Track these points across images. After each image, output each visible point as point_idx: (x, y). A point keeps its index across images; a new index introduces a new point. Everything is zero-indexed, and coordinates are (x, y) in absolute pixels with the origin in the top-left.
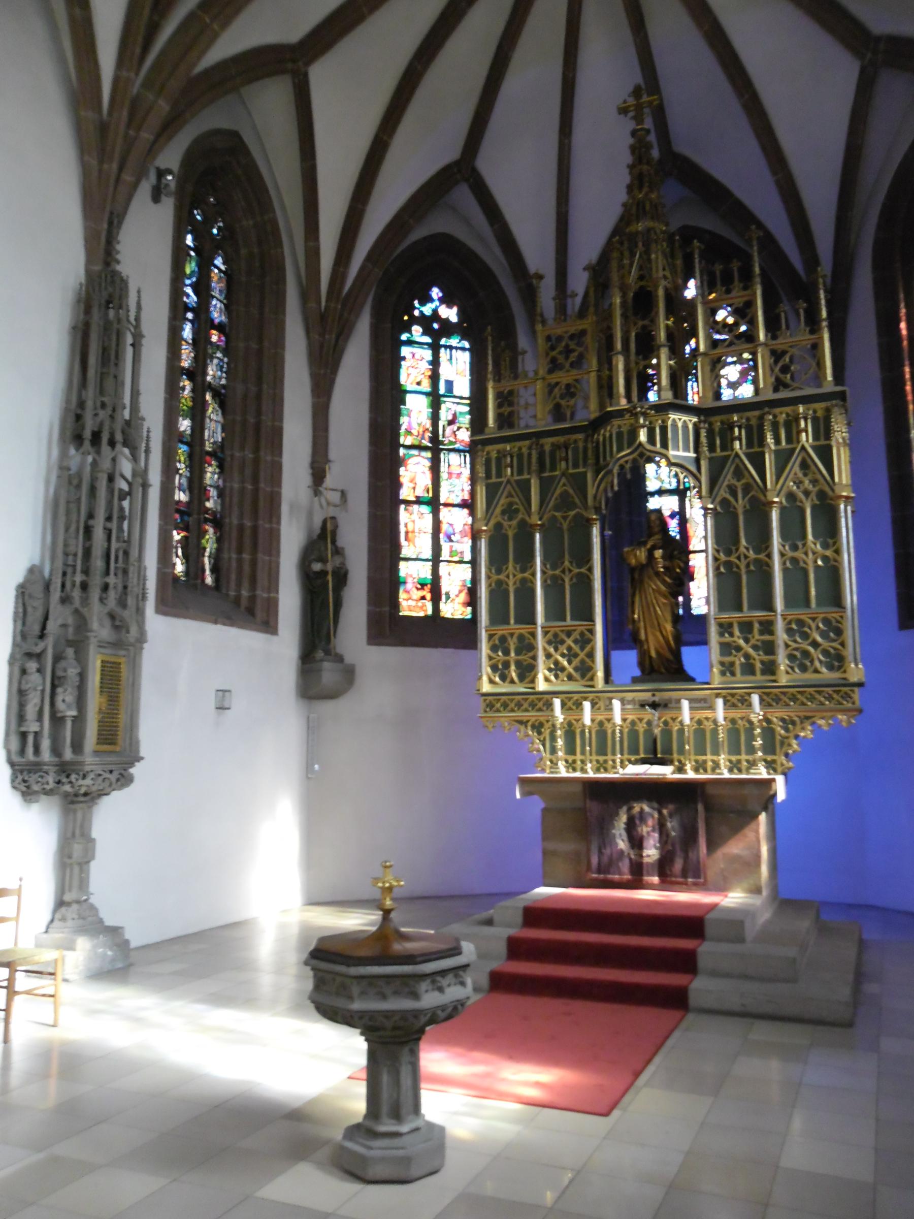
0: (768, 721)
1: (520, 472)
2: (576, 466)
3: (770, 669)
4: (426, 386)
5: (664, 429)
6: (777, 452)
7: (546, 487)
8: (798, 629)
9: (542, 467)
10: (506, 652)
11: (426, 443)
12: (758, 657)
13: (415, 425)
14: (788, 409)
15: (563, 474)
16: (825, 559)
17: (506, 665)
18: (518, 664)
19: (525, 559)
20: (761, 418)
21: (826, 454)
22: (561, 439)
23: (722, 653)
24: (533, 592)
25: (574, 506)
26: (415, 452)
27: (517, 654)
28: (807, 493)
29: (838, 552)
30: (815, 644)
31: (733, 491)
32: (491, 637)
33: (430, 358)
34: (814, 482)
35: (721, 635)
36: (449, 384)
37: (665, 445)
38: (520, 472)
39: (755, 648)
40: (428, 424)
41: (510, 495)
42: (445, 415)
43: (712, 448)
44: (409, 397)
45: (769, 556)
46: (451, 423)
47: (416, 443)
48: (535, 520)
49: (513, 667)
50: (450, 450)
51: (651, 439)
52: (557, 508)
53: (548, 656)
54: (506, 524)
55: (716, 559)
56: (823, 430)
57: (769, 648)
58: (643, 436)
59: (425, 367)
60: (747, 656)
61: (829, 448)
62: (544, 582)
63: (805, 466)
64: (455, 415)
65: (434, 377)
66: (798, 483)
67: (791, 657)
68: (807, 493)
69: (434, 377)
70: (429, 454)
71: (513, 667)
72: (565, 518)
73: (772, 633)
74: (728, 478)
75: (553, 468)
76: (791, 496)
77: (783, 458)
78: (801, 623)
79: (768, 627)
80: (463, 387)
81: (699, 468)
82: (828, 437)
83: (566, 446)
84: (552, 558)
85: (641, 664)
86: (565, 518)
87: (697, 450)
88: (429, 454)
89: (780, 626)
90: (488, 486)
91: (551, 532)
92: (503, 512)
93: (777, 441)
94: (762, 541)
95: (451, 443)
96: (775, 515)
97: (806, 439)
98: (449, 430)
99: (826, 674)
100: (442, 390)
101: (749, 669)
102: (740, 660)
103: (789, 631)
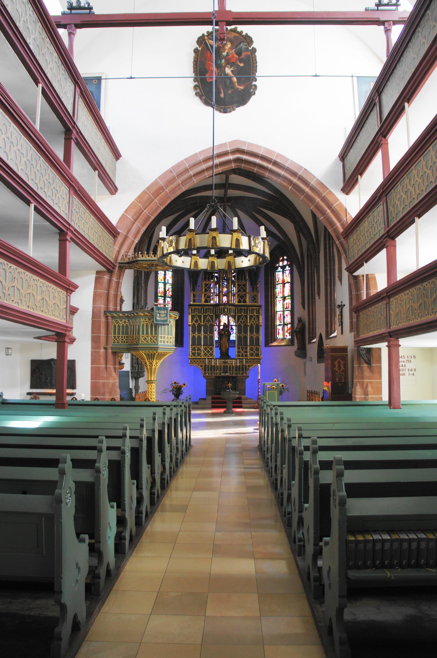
0: (246, 366)
1: (199, 313)
2: (211, 313)
3: (246, 356)
4: (163, 281)
5: (230, 309)
6: (250, 316)
7: (205, 317)
8: (251, 349)
9: (204, 313)
10: (195, 351)
11: (163, 295)
12: (244, 354)
13: (161, 291)
14: (252, 307)
15: (208, 315)
16: (257, 336)
17: (195, 353)
18: (197, 353)
19: (200, 332)
20: (247, 309)
21: (258, 317)
22: (208, 307)
23: (238, 353)
24: (201, 338)
25: (210, 322)
26: (161, 298)
27: (208, 353)
28: (254, 324)
29: (259, 335)
30: (254, 352)
31: (241, 322)
32: (192, 347)
33: (164, 274)
34: (256, 322)
35: (238, 349)
36: (168, 280)
37: (230, 312)
38: (199, 313)
39: (244, 352)
40: (163, 290)
41: (196, 318)
42: (167, 289)
43: (238, 314)
44: (159, 284)
45: (247, 335)
46: (168, 290)
47: (161, 295)
48: (202, 324)
49: (196, 354)
50: (168, 297)
51: (228, 311)
52: (206, 322)
53: (204, 352)
54: (195, 324)
55: (238, 335)
56: (258, 312)
57: (246, 352)
58: (226, 311)
59: (163, 276)
60: (242, 353)
61: (259, 316)
62: (203, 337)
63: (254, 319)
64: (169, 288)
65: (165, 278)
66: (253, 322)
67: (250, 354)
68: (254, 324)
69: (165, 278)
70: (163, 298)
71: (196, 354)
72: (208, 324)
73: (247, 349)
74: (241, 320)
75: (206, 313)
76: (252, 324)
77: (251, 317)
78: (252, 348)
79: (246, 348)
80: (170, 281)
81: (235, 317)
82: (259, 314)
83: (209, 309)
84: (205, 332)
85: (221, 354)
86: (208, 324)
87: (235, 313)
88: (163, 298)
89: (248, 348)
90: (192, 315)
91: (205, 326)
92: (195, 321)
93: (250, 314)
94: (246, 332)
95: (168, 295)
96: (249, 328)
97: (255, 314)
98: (168, 292)
99: (256, 357)
100: (166, 282)
101: (242, 356)
102: (241, 354)
103: (250, 349)
